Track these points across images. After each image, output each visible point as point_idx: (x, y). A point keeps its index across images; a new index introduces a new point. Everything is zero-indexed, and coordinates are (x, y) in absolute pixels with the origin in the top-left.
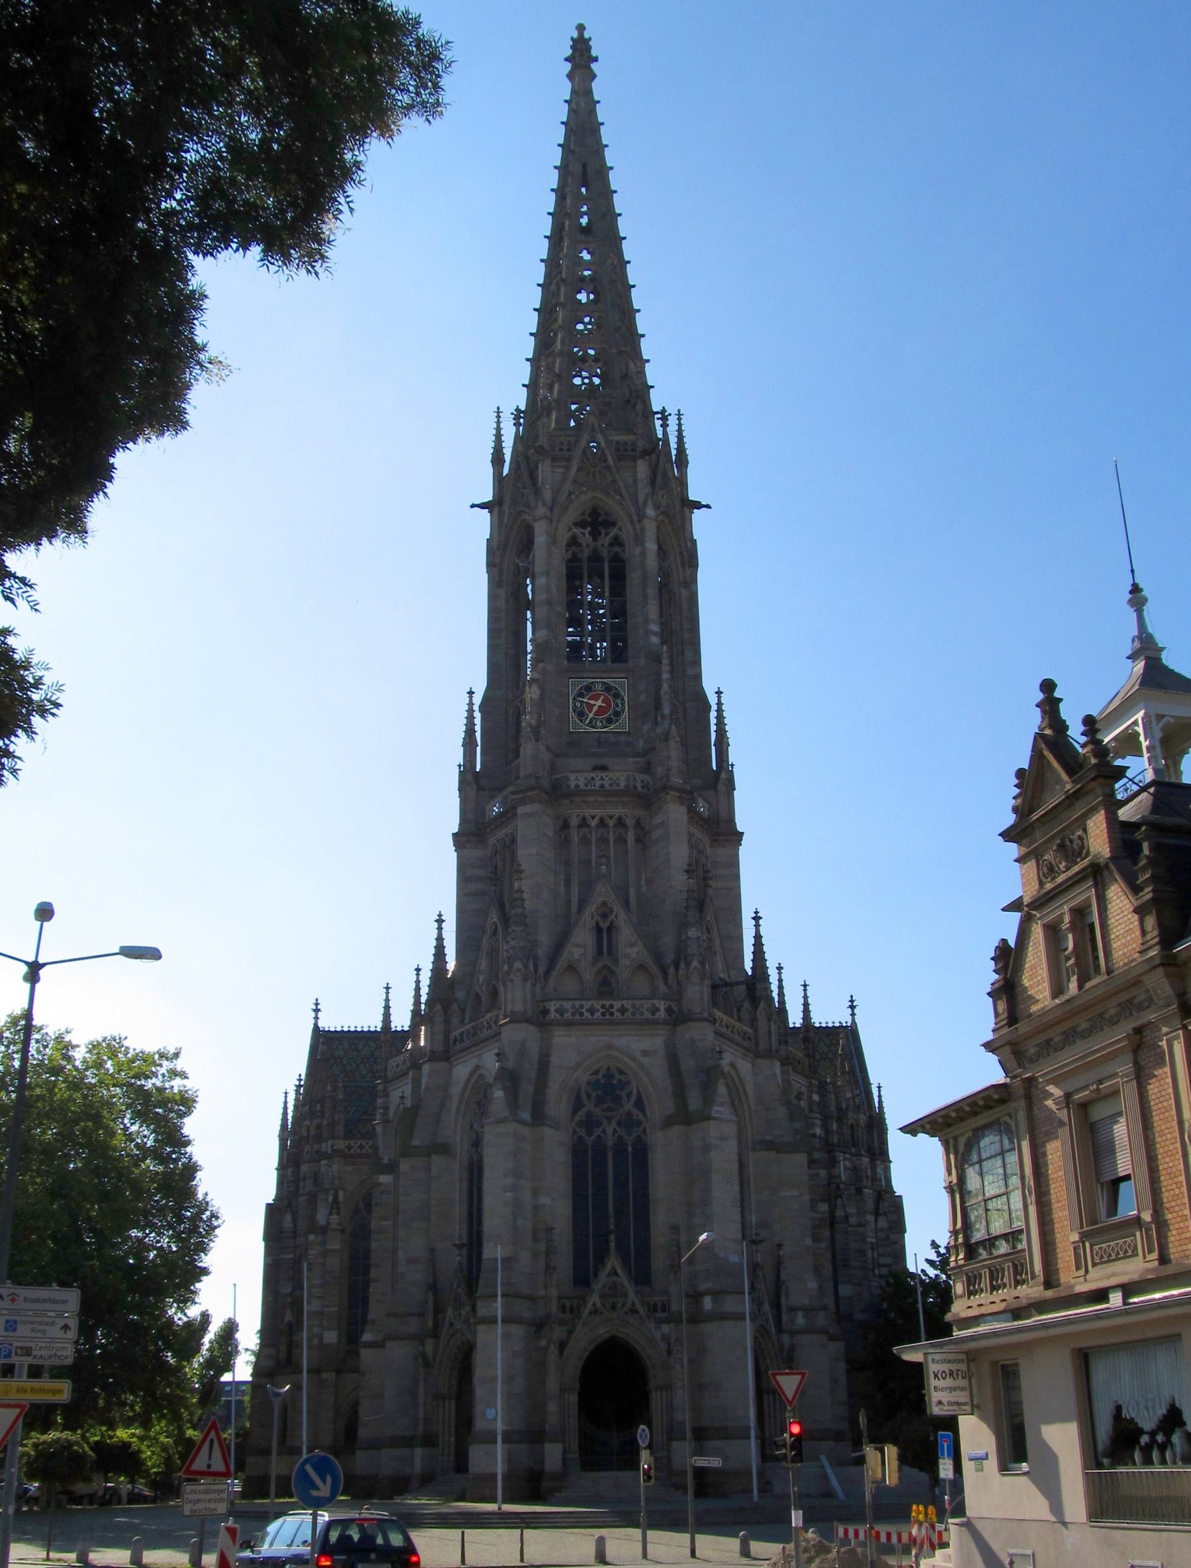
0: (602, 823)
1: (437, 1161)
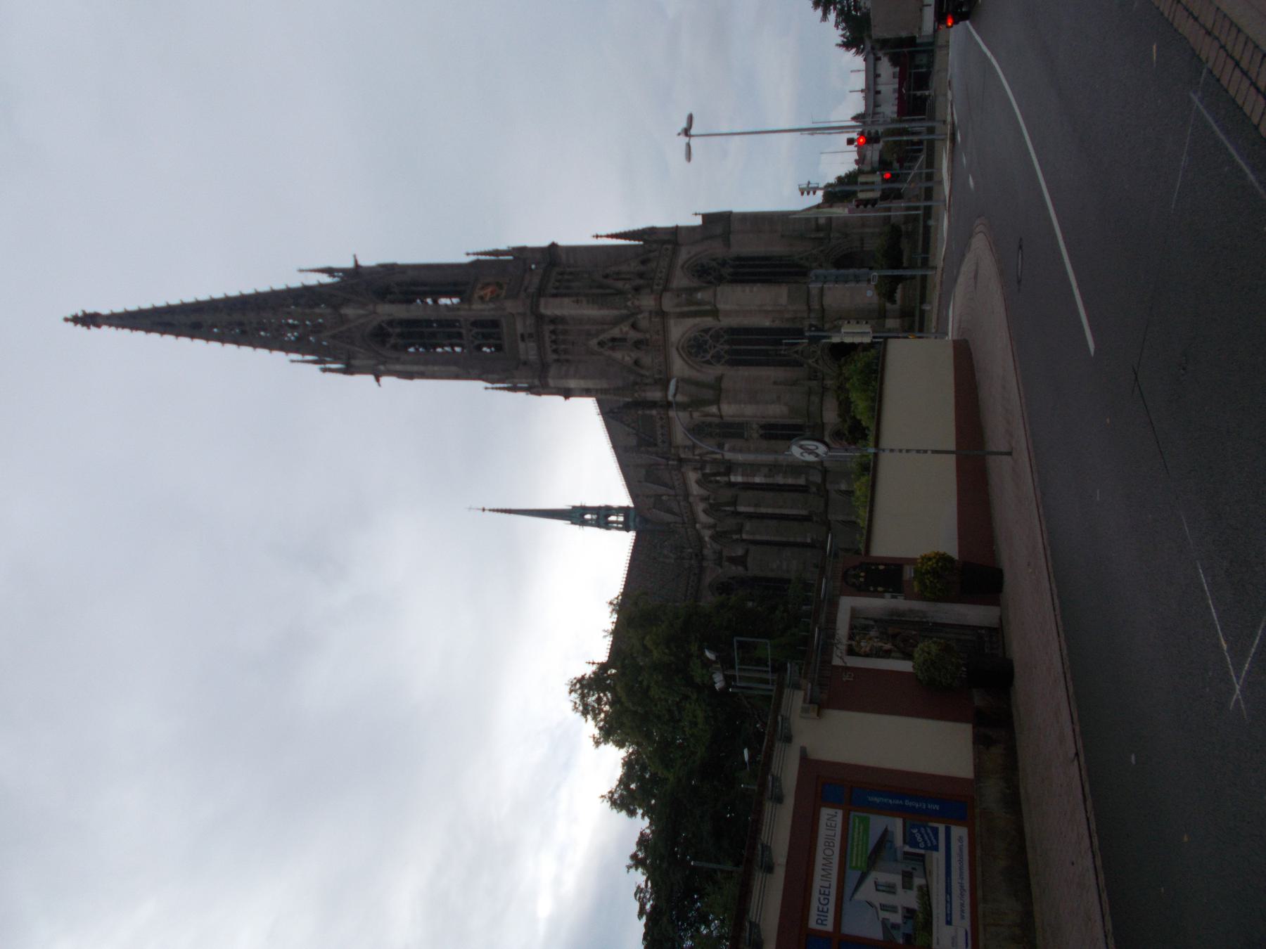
0: (559, 281)
1: (725, 385)
